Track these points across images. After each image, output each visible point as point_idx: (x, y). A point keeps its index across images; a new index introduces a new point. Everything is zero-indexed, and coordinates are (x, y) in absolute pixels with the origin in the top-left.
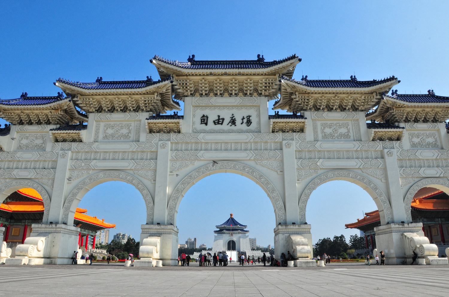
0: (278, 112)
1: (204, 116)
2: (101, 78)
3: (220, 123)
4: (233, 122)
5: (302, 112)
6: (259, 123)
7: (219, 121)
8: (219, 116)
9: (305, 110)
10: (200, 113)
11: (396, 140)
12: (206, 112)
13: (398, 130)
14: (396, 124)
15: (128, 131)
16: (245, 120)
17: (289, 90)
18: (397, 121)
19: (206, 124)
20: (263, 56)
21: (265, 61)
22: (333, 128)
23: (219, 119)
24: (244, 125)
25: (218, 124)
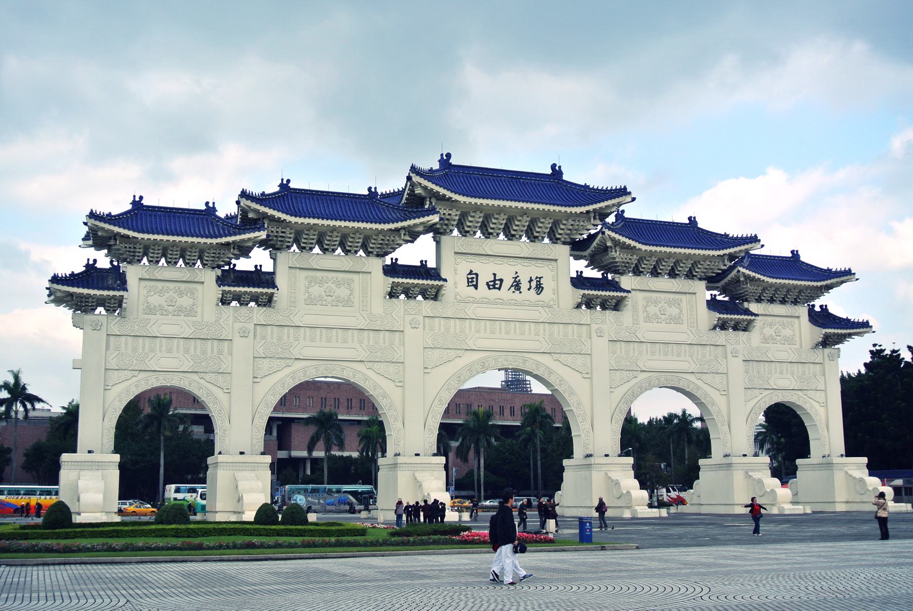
0: (581, 272)
1: (471, 273)
2: (288, 181)
3: (497, 286)
4: (517, 285)
5: (617, 276)
6: (556, 291)
7: (495, 284)
8: (495, 275)
9: (622, 274)
10: (465, 266)
11: (743, 330)
12: (477, 266)
13: (749, 317)
14: (746, 305)
15: (348, 292)
16: (534, 284)
17: (609, 244)
18: (747, 300)
19: (476, 287)
20: (560, 167)
21: (565, 178)
22: (660, 305)
23: (495, 280)
24: (533, 291)
25: (495, 288)
